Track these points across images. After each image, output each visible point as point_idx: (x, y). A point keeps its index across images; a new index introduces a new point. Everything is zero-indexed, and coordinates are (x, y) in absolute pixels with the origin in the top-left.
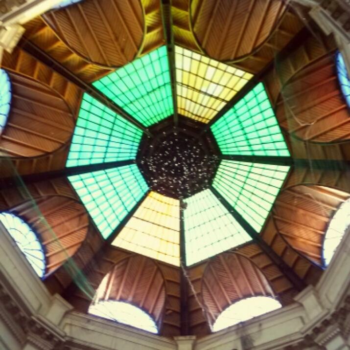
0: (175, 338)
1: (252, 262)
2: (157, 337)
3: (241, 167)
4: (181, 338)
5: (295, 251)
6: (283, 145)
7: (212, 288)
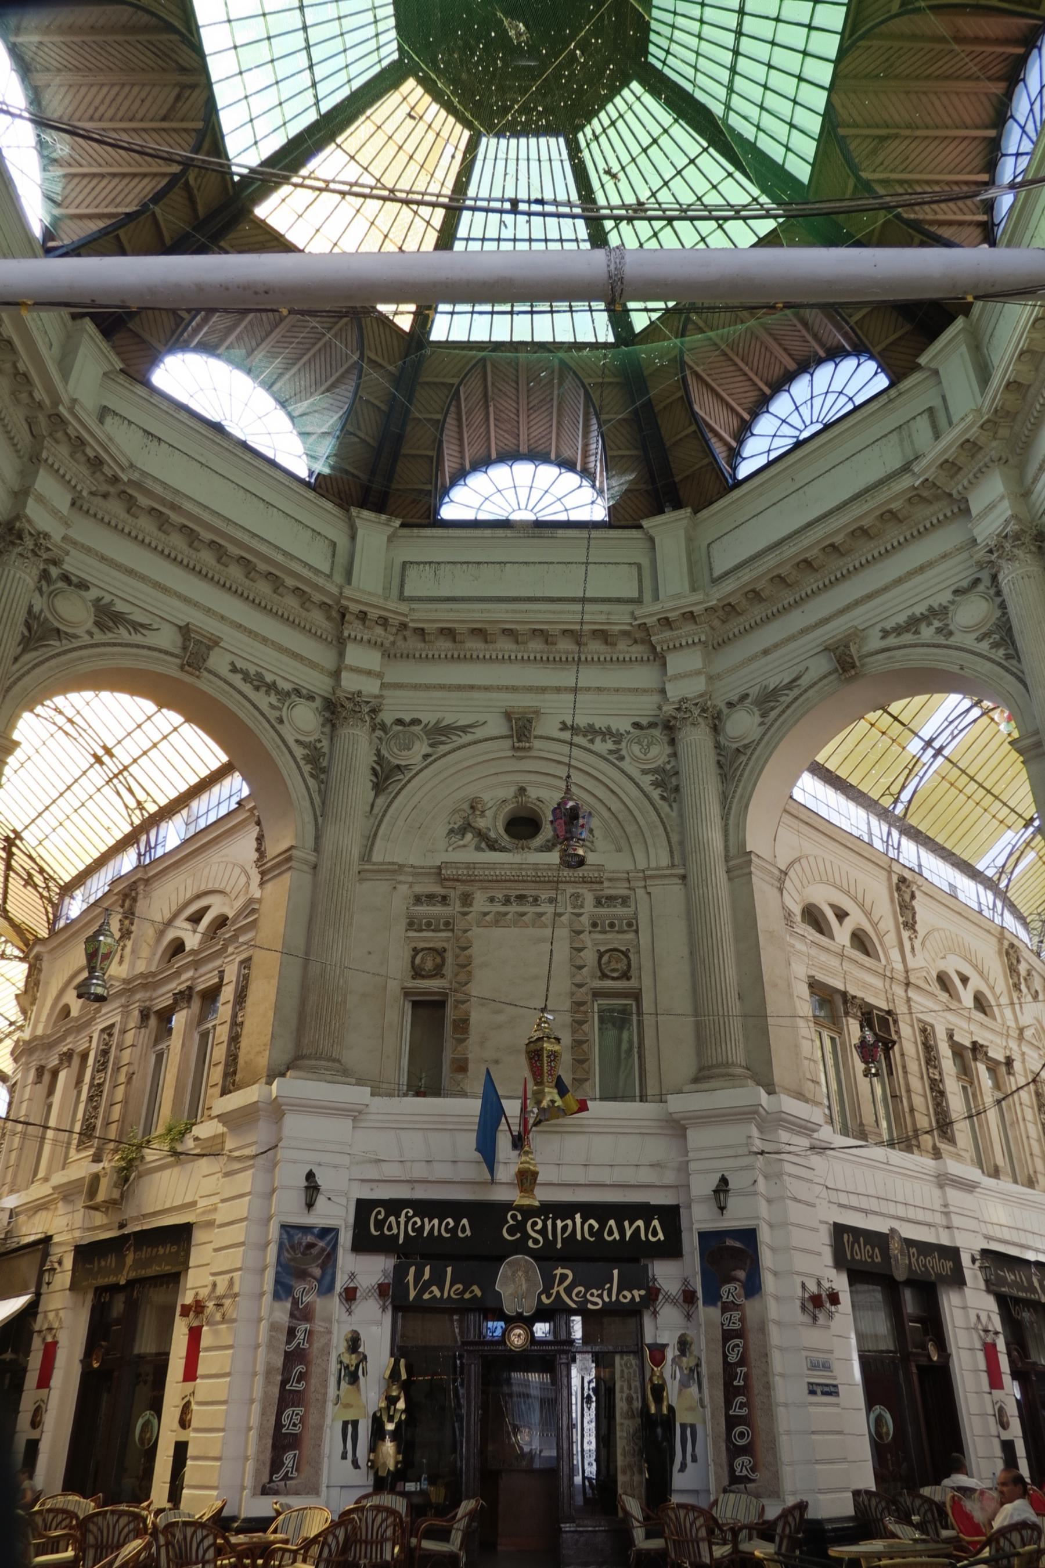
0: (354, 511)
1: (586, 392)
2: (311, 495)
3: (677, 131)
4: (366, 514)
5: (694, 414)
6: (808, 148)
7: (469, 413)
